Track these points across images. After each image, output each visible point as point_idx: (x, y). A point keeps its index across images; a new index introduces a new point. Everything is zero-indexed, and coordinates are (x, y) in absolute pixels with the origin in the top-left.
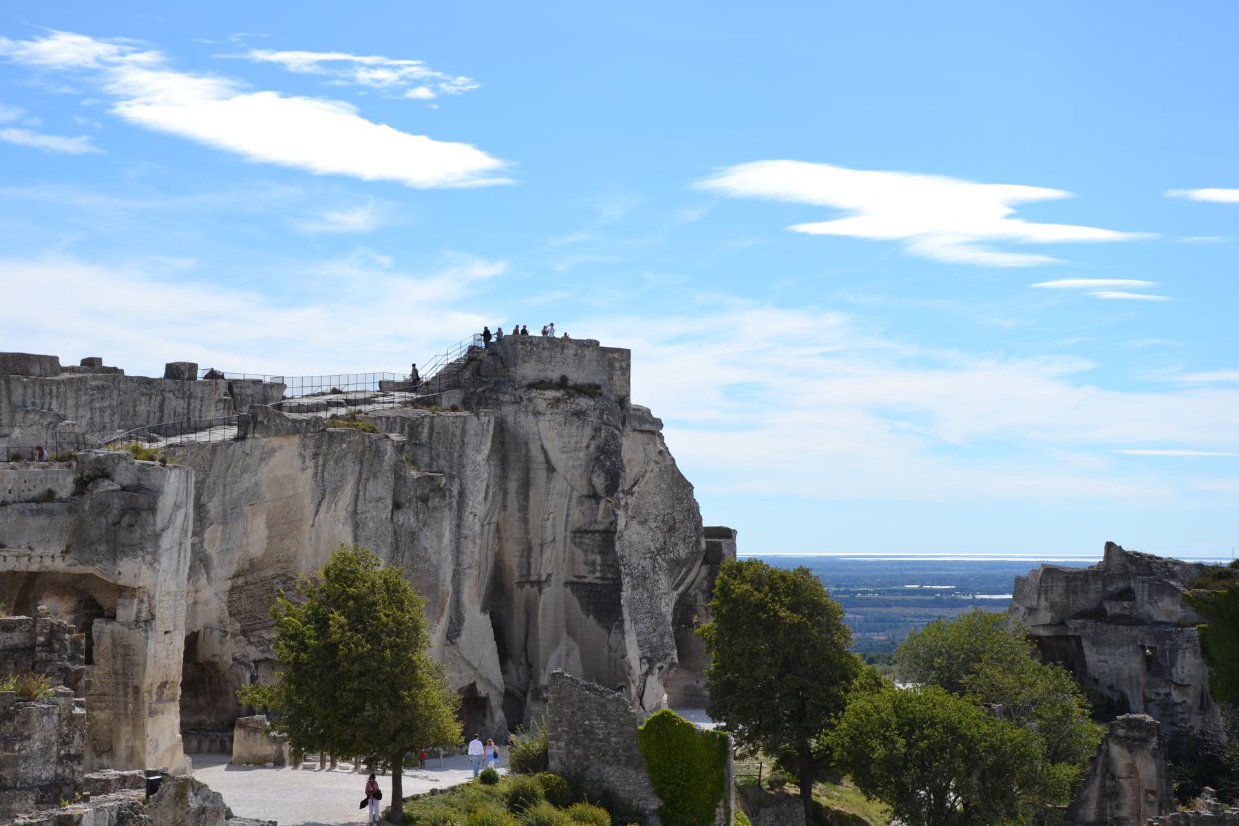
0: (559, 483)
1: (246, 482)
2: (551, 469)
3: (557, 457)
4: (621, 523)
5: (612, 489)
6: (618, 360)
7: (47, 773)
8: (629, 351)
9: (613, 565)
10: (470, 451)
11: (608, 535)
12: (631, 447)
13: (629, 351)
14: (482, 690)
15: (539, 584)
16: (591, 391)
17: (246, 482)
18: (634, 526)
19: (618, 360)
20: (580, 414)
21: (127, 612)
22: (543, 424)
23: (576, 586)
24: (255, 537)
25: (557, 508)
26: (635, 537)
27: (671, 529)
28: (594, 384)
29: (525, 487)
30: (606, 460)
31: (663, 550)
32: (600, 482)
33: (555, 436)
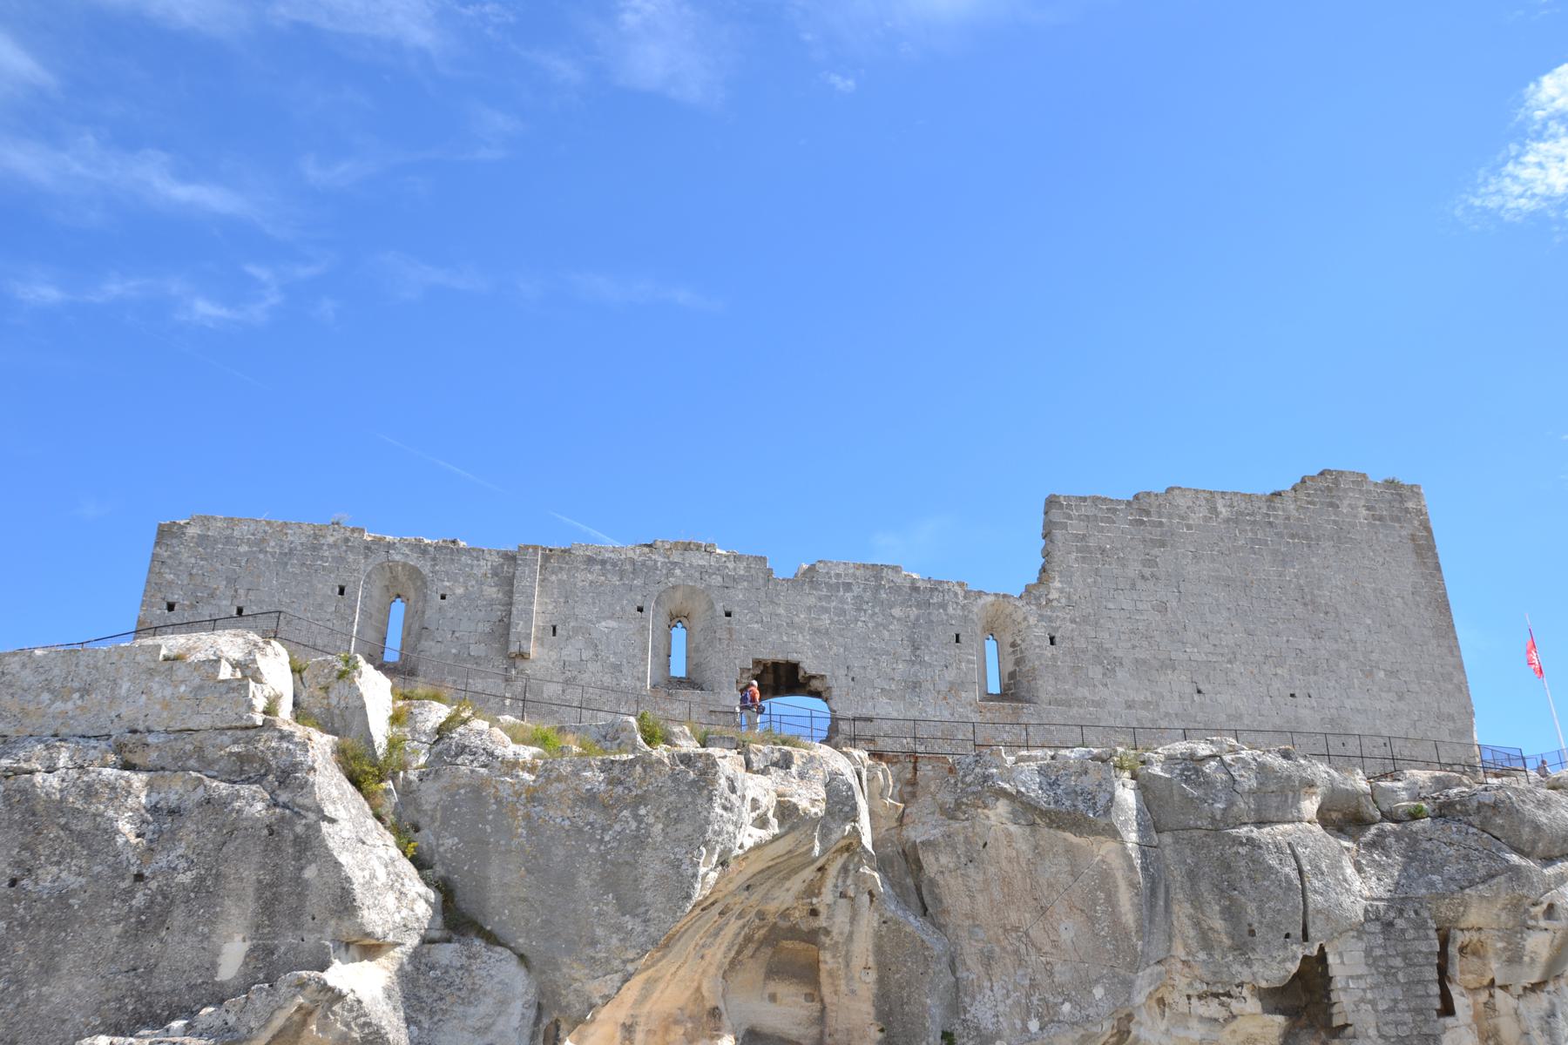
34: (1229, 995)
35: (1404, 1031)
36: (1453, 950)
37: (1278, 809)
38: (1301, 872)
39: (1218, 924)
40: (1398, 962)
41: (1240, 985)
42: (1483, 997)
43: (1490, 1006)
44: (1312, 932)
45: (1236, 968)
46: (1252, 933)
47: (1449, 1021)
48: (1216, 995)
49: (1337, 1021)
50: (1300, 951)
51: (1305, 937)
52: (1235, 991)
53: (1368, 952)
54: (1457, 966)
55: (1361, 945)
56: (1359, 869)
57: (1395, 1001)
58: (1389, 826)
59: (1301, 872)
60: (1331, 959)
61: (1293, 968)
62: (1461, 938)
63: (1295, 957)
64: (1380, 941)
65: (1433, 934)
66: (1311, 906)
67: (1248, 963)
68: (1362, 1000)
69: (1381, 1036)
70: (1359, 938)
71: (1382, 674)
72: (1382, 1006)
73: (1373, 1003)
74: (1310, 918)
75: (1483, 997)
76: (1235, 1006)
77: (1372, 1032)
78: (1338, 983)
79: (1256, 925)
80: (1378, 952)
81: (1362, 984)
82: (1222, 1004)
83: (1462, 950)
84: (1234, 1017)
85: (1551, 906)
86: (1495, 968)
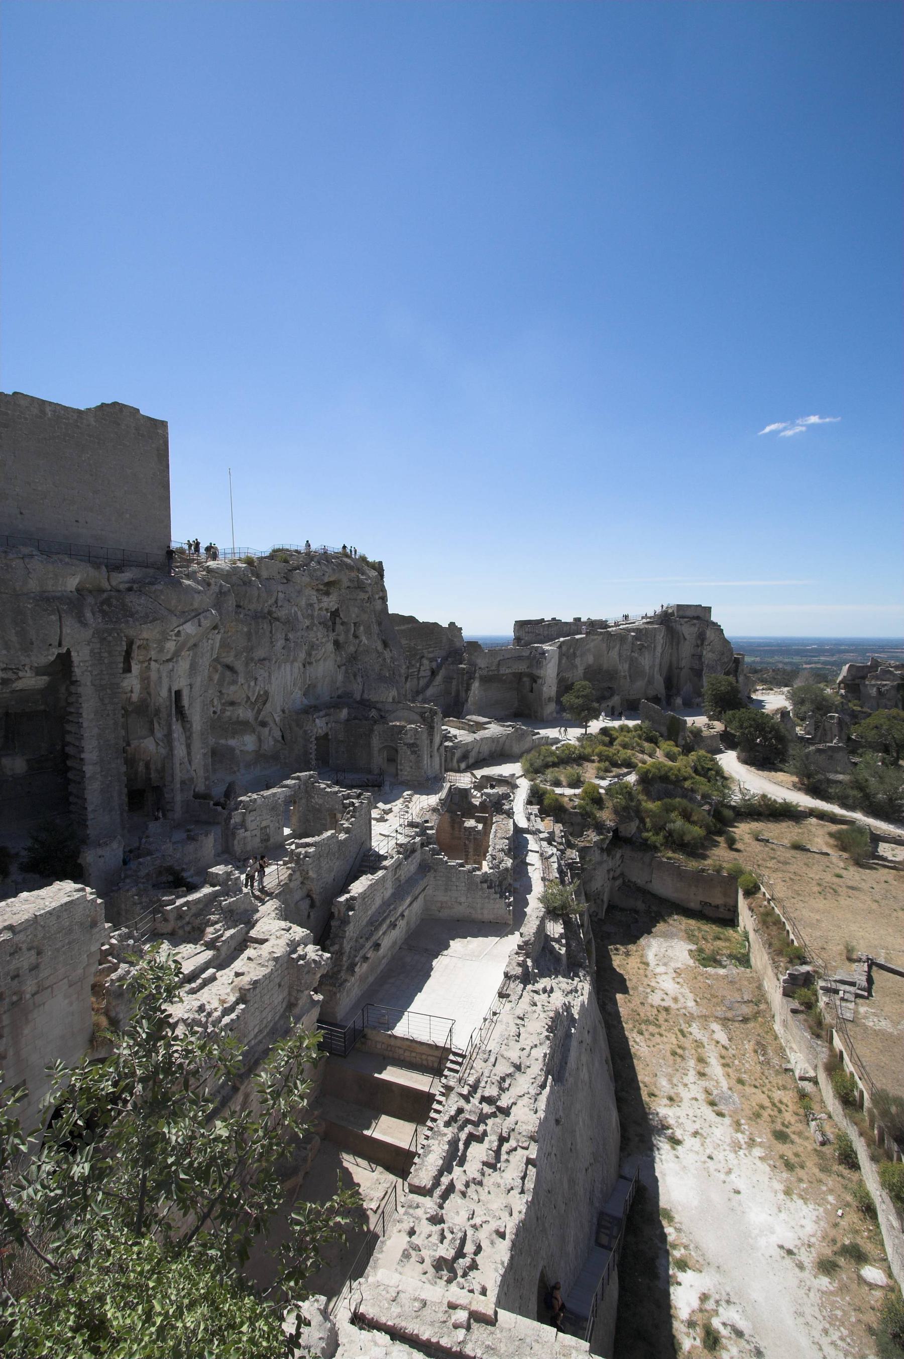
0: (687, 643)
1: (587, 647)
2: (685, 639)
3: (687, 637)
4: (704, 653)
5: (702, 644)
6: (708, 610)
7: (412, 742)
8: (710, 608)
9: (702, 664)
10: (657, 637)
11: (700, 657)
12: (710, 634)
13: (710, 608)
14: (659, 696)
15: (681, 669)
16: (698, 618)
17: (587, 647)
18: (710, 654)
19: (708, 610)
20: (694, 625)
21: (539, 681)
22: (683, 628)
23: (692, 669)
24: (590, 659)
25: (686, 649)
26: (708, 656)
27: (723, 654)
28: (698, 616)
29: (678, 644)
30: (701, 637)
31: (720, 659)
32: (699, 642)
33: (688, 631)
34: (18, 669)
35: (104, 682)
36: (135, 647)
37: (53, 586)
38: (60, 617)
39: (14, 639)
40: (106, 655)
41: (24, 665)
42: (147, 664)
43: (148, 668)
44: (64, 643)
45: (22, 658)
46: (32, 643)
47: (129, 675)
48: (12, 669)
49: (74, 679)
50: (56, 651)
51: (60, 645)
52: (21, 668)
53: (92, 651)
54: (135, 653)
55: (89, 648)
56: (94, 614)
57: (102, 671)
58: (113, 593)
59: (60, 617)
60: (73, 654)
61: (52, 658)
62: (138, 643)
63: (53, 654)
64: (98, 646)
65: (124, 643)
66: (64, 632)
67: (29, 656)
68: (86, 671)
69: (93, 685)
70: (88, 644)
71: (128, 516)
72: (95, 673)
73: (91, 672)
74: (63, 637)
75: (147, 664)
76: (21, 674)
77: (89, 684)
78: (76, 664)
79: (34, 640)
80: (96, 651)
81: (87, 664)
82: (14, 673)
83: (139, 647)
84: (20, 678)
85: (179, 631)
86: (153, 654)
